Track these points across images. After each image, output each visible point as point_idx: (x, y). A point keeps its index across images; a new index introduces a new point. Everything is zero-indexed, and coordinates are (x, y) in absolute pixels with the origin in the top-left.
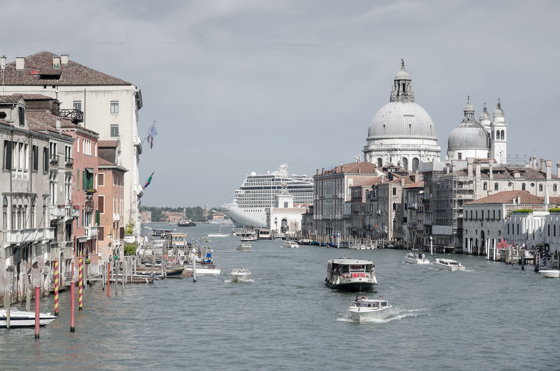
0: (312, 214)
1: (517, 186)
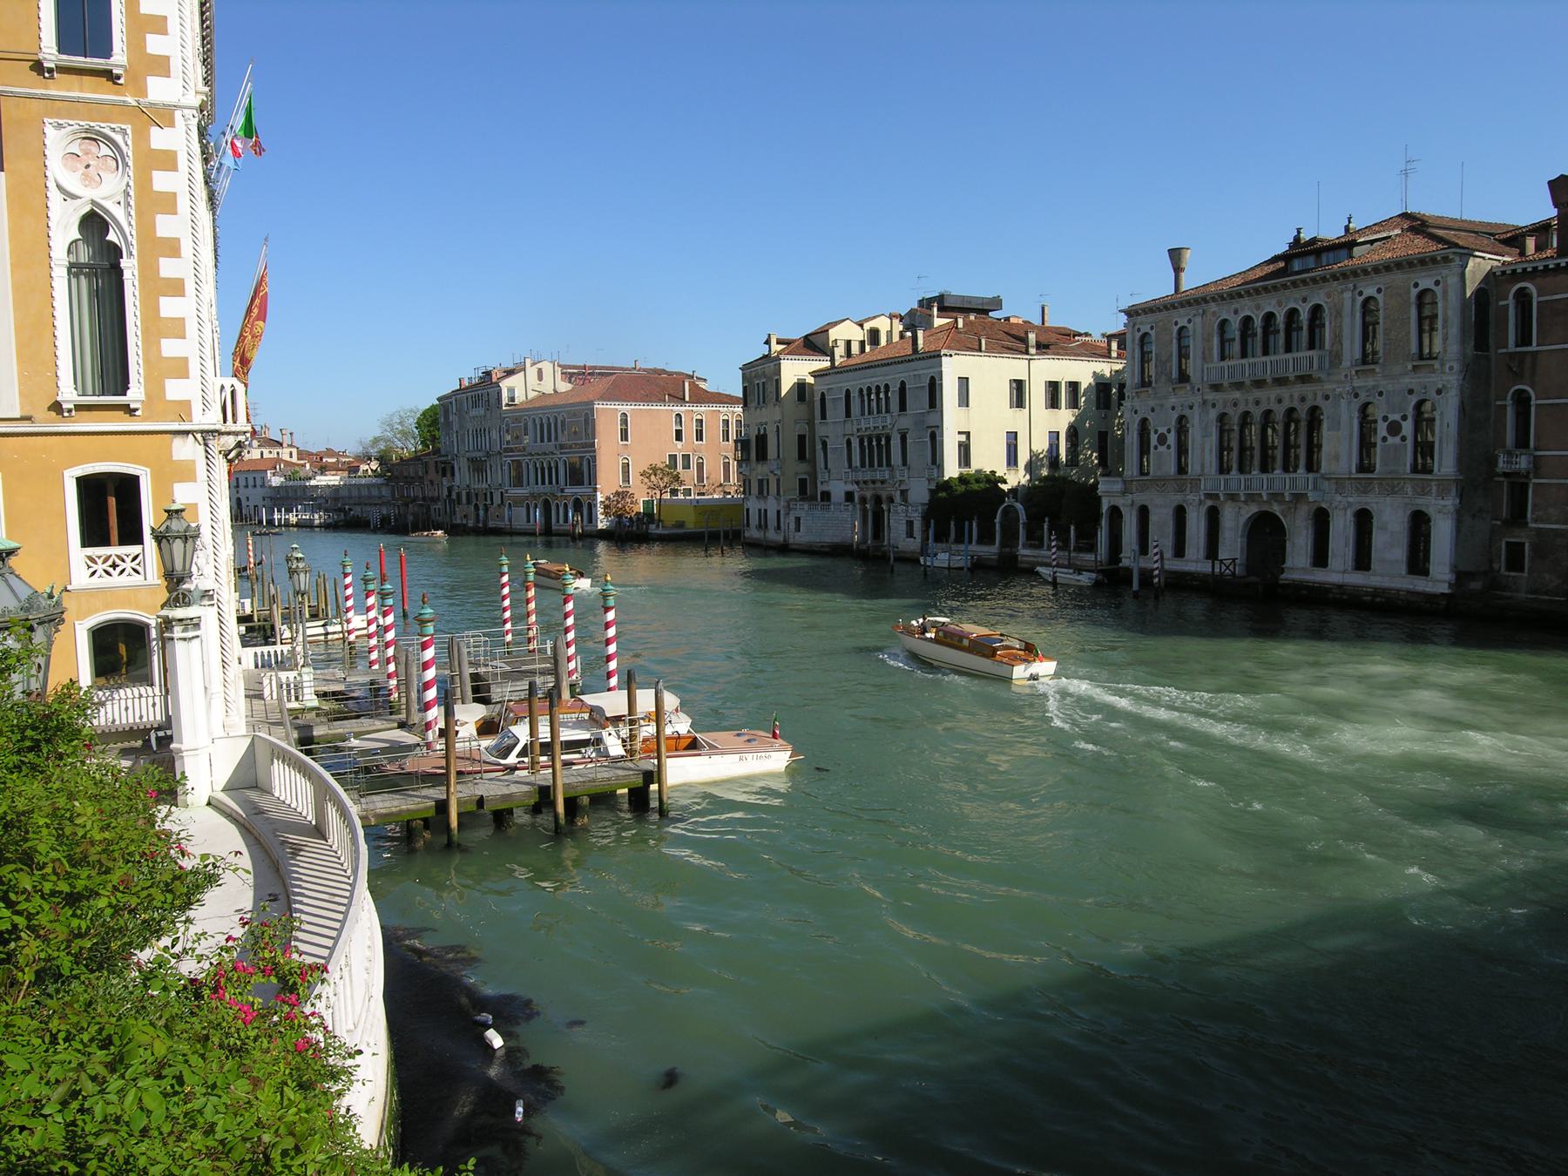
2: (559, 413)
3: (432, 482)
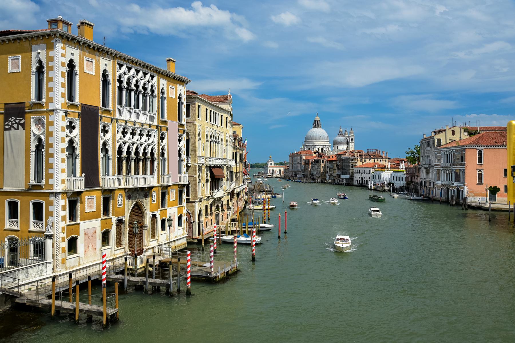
1: (373, 161)
2: (453, 150)
3: (417, 176)
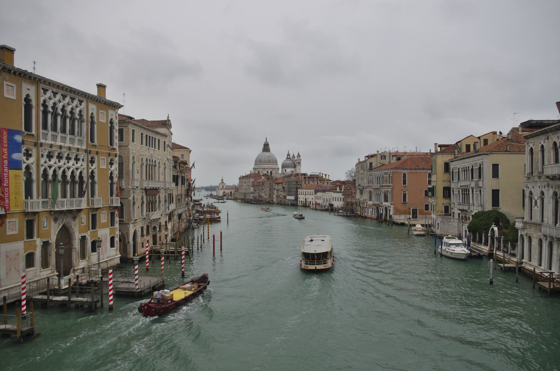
0: (238, 191)
2: (382, 173)
3: (353, 196)
